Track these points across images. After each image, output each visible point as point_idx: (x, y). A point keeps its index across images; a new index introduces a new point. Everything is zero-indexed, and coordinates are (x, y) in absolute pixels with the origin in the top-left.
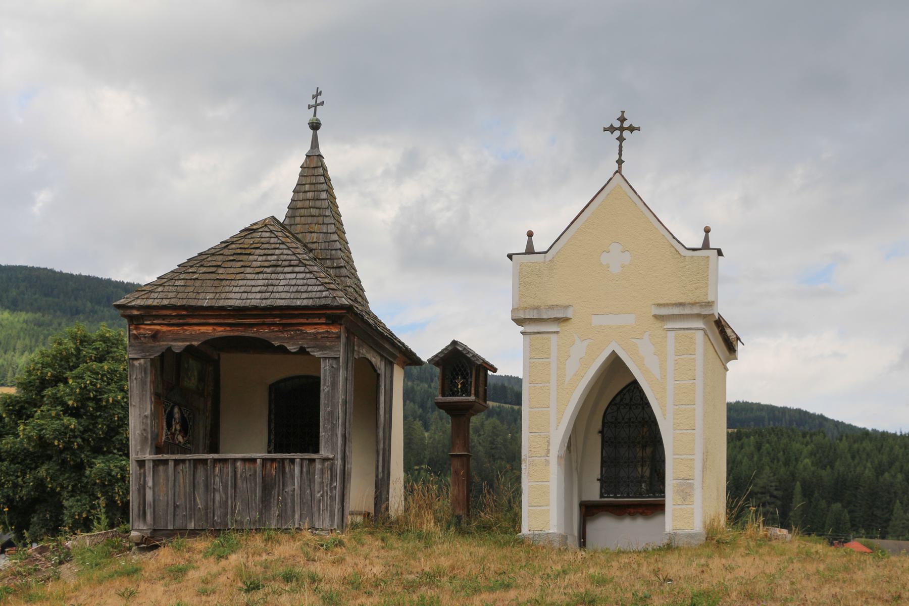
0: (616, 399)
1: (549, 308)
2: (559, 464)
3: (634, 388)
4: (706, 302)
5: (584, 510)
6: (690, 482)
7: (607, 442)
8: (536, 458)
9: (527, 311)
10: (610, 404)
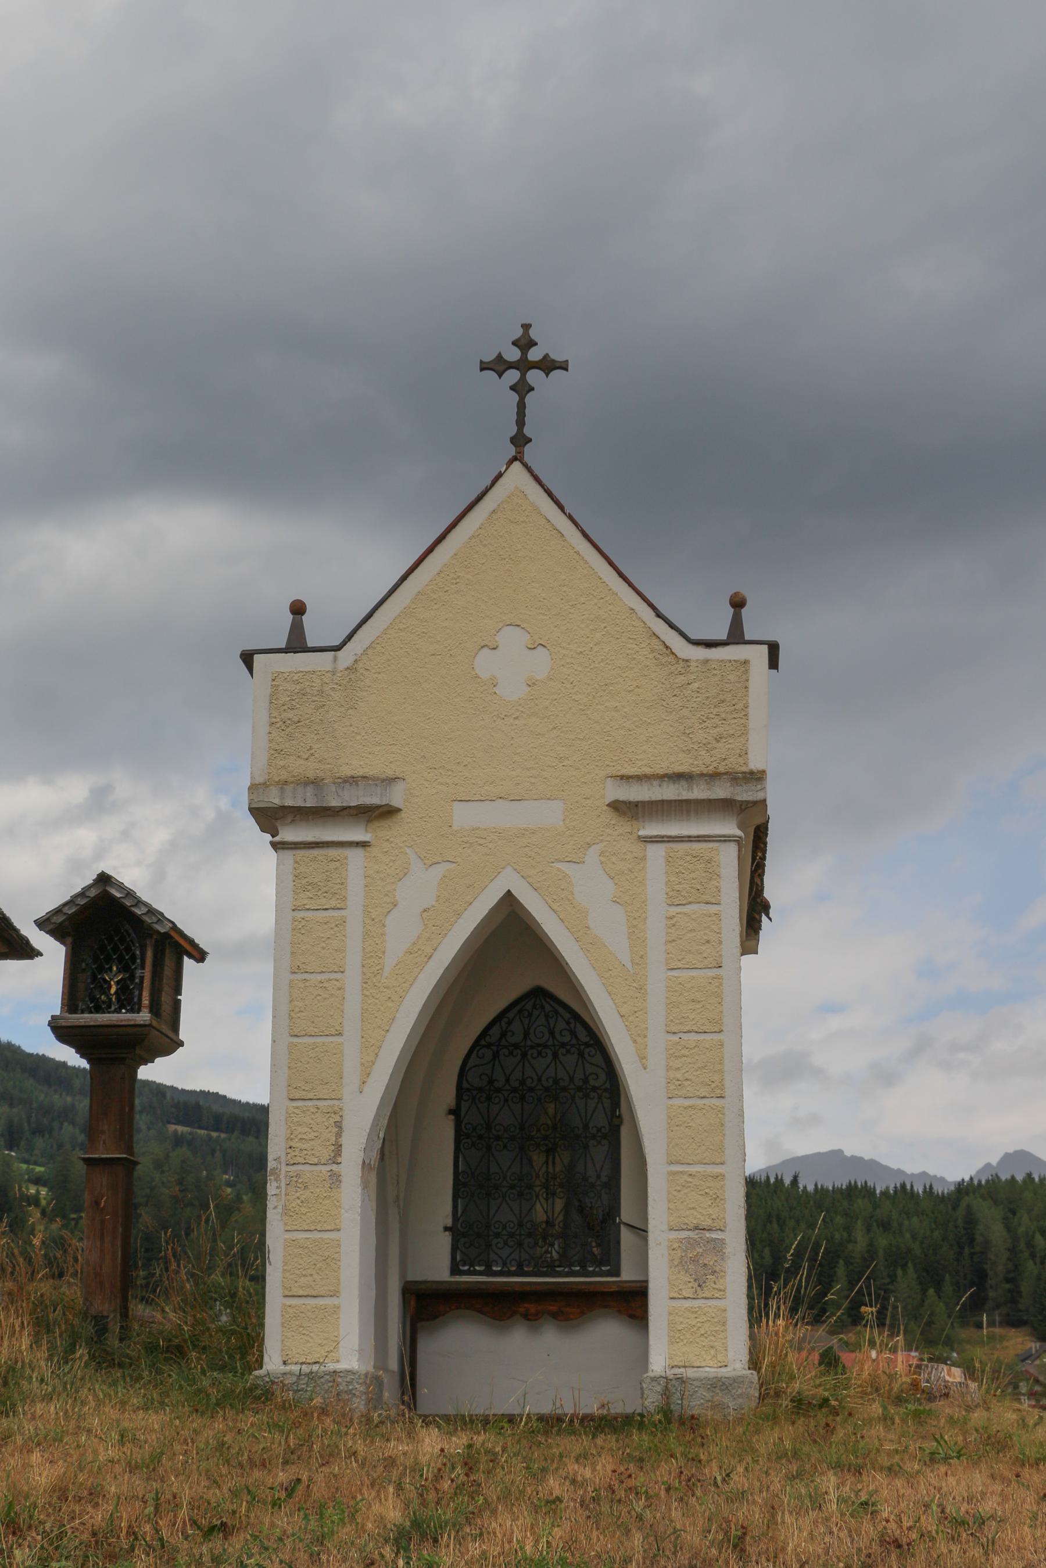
0: (491, 1032)
1: (345, 782)
2: (365, 1184)
3: (534, 1007)
4: (744, 773)
5: (413, 1303)
6: (714, 1235)
7: (468, 1136)
8: (307, 1168)
9: (289, 788)
10: (476, 1043)
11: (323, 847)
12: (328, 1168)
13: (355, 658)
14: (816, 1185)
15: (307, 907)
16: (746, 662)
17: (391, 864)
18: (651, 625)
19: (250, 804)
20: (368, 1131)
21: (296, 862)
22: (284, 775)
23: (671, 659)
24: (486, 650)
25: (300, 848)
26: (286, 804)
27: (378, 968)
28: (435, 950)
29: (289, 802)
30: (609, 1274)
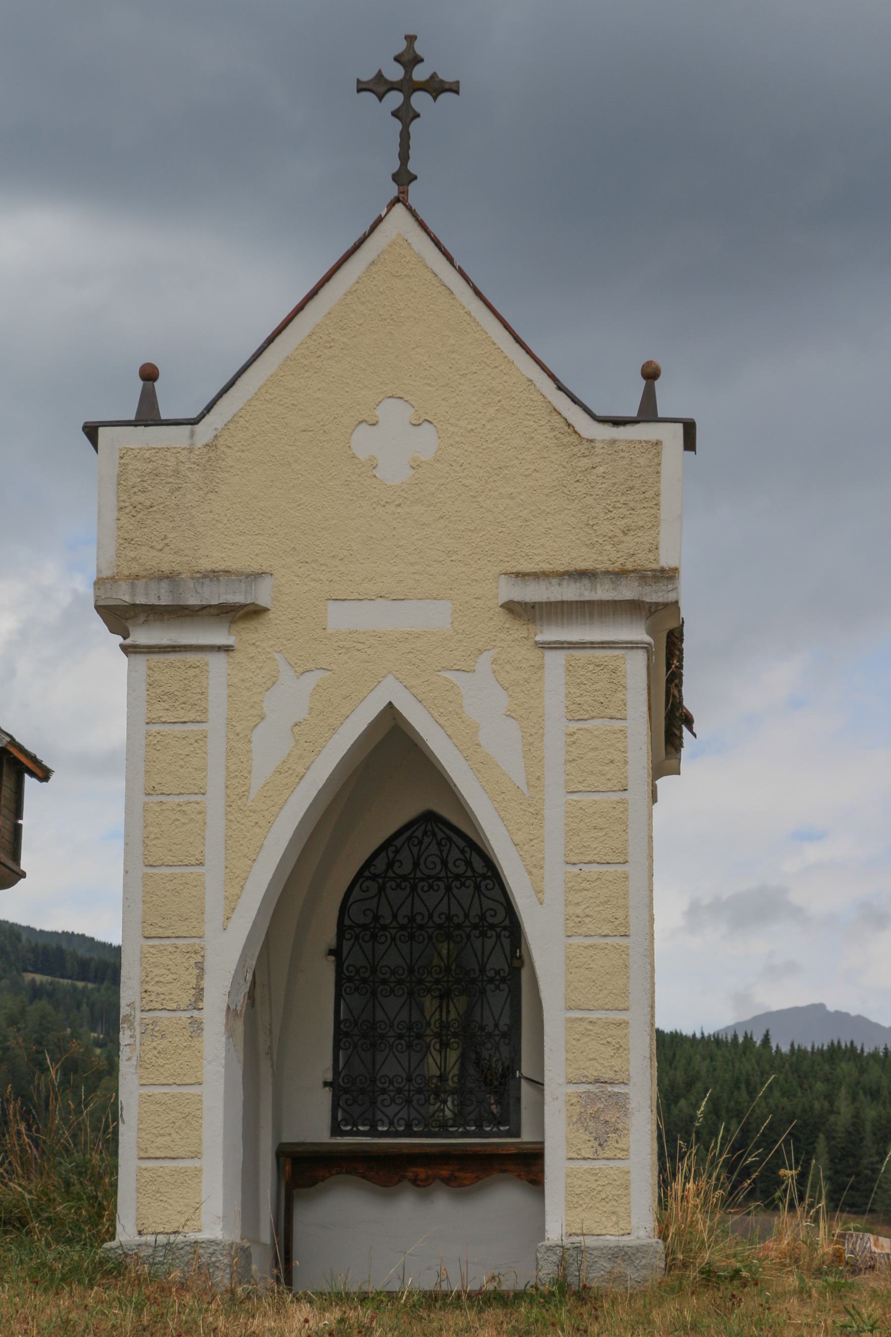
0: (377, 862)
1: (205, 576)
2: (230, 1033)
3: (425, 833)
7: (350, 979)
11: (180, 651)
12: (188, 1014)
13: (215, 433)
14: (792, 1045)
15: (163, 720)
16: (658, 443)
17: (258, 671)
18: (550, 399)
19: (96, 601)
20: (233, 972)
21: (150, 668)
22: (135, 569)
23: (573, 438)
24: (364, 425)
25: (154, 652)
26: (138, 602)
27: (243, 789)
28: (307, 769)
29: (141, 600)
30: (508, 1134)
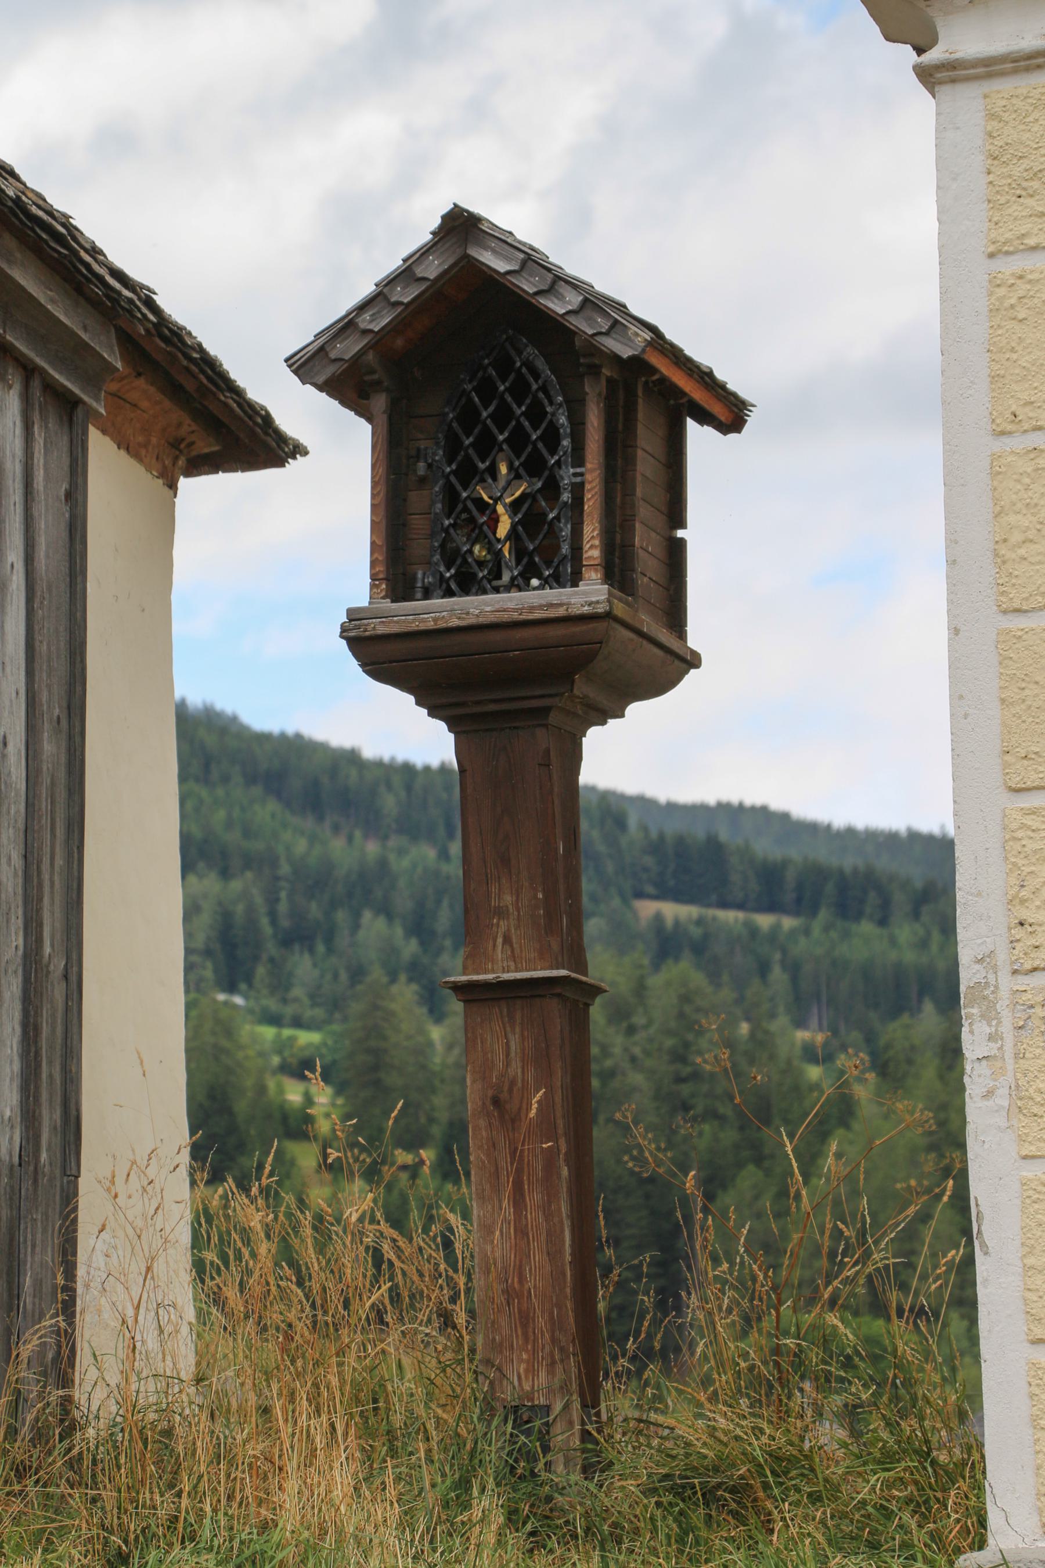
15: (1031, 242)
21: (992, 116)
25: (1002, 74)
